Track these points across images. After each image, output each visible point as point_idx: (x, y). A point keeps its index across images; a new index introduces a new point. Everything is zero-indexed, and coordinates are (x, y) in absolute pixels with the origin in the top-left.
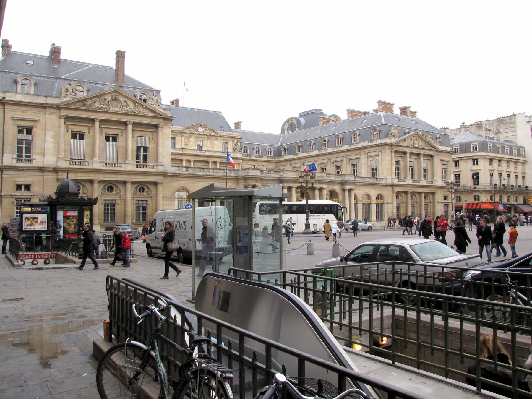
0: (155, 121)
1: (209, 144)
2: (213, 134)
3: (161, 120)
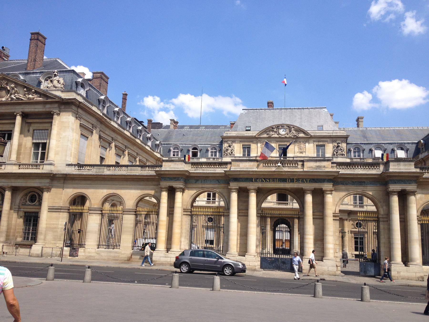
0: (48, 108)
1: (297, 149)
2: (302, 135)
3: (56, 105)
